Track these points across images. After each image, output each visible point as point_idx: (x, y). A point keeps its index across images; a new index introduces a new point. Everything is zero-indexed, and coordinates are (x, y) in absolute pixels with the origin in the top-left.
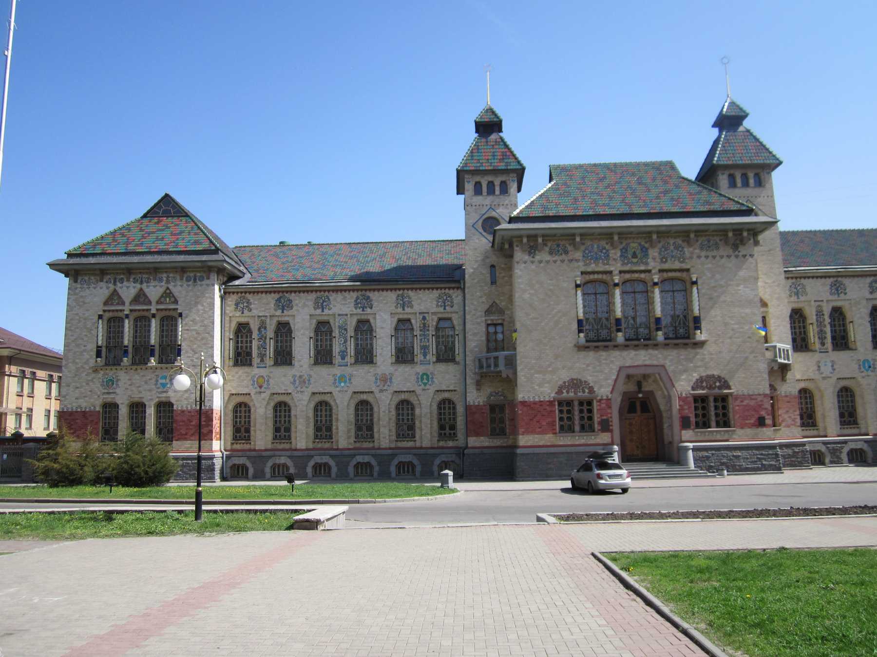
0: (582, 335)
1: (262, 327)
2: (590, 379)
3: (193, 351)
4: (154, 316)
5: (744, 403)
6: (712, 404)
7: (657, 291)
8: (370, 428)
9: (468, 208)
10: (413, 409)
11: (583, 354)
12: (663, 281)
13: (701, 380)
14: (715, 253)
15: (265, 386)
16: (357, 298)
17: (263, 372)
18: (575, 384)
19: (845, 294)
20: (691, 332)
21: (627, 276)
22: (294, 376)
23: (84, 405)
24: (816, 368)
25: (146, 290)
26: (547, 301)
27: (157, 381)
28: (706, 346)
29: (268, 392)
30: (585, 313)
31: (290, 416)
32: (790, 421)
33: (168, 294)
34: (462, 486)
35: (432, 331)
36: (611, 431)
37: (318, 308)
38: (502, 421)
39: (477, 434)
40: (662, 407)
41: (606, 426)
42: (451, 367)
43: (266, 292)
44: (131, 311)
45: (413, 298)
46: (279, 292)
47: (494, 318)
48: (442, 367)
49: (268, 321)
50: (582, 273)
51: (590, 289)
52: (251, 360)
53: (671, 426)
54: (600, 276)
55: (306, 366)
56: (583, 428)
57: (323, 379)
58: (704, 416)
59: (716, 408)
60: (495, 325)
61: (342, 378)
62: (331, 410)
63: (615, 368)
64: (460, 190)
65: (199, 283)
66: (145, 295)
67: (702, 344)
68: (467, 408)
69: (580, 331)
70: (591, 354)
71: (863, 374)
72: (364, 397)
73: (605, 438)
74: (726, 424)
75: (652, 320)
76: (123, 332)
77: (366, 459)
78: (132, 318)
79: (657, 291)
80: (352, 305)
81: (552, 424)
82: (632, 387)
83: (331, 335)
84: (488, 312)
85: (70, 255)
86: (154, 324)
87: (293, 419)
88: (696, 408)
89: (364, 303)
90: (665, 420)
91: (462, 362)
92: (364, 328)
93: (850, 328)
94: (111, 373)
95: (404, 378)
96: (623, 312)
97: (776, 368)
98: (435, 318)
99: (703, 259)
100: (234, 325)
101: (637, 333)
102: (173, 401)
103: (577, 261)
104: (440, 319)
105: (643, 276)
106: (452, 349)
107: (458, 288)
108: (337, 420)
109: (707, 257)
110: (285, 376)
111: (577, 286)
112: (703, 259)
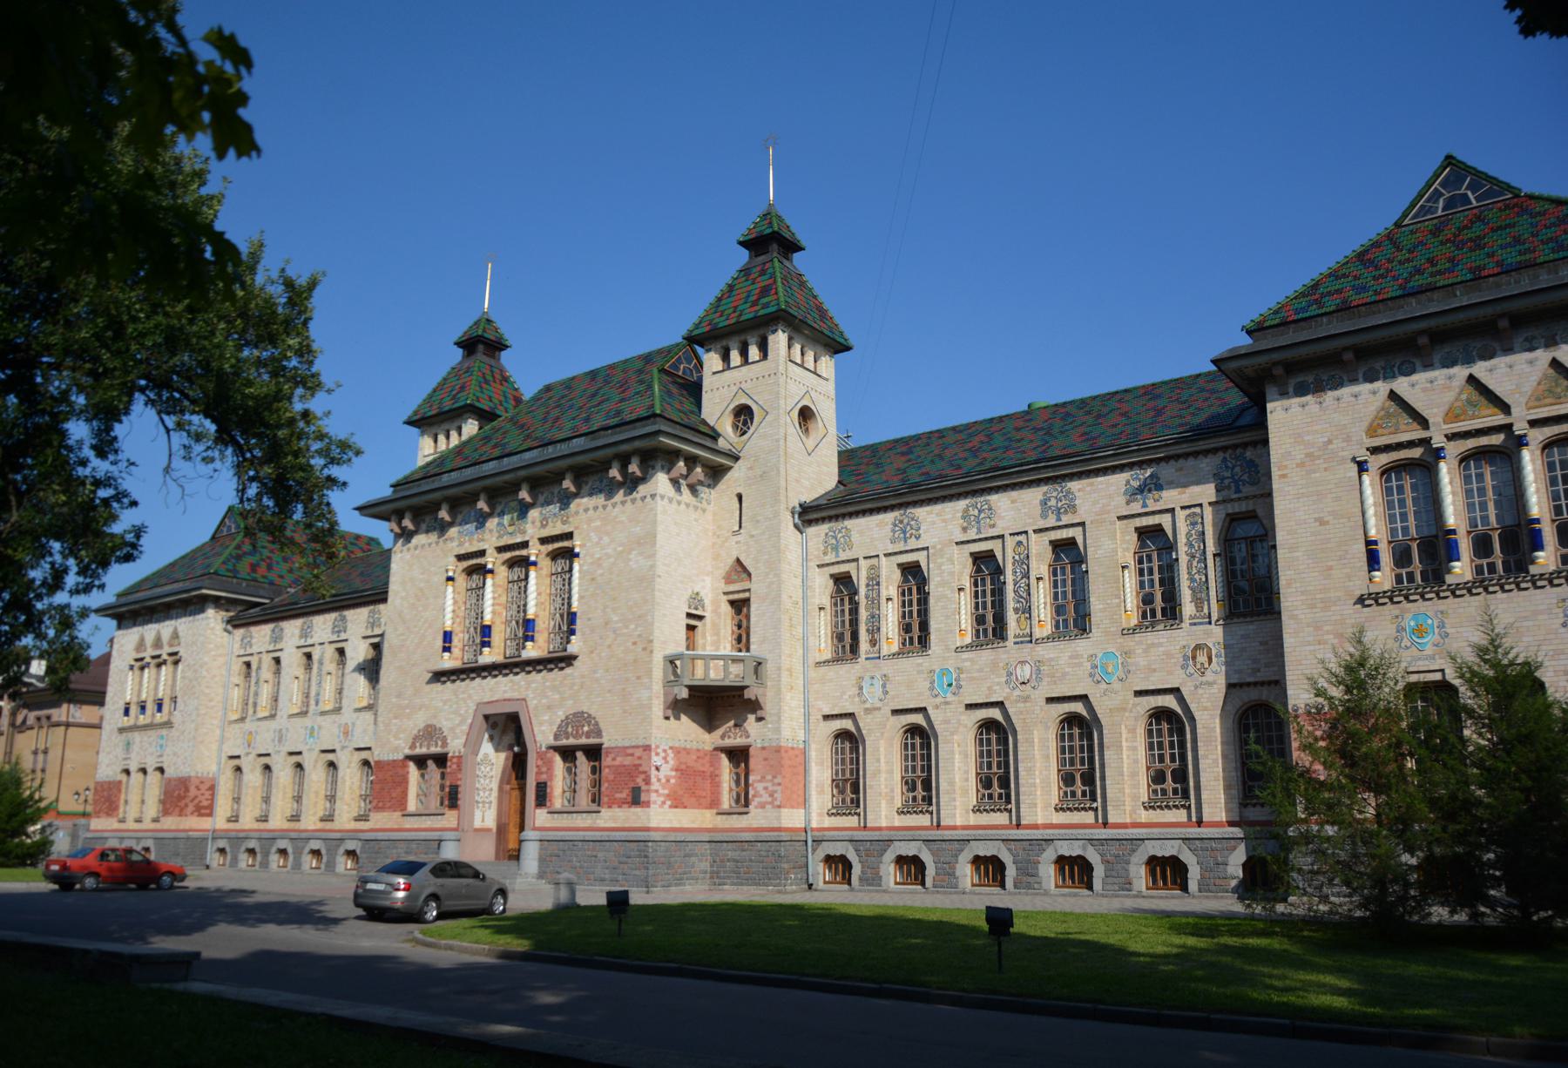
2: (445, 724)
5: (617, 763)
13: (567, 721)
18: (430, 732)
19: (918, 538)
24: (855, 690)
28: (576, 663)
32: (766, 798)
71: (939, 700)
85: (119, 596)
99: (591, 512)
103: (452, 539)
109: (596, 508)
111: (450, 579)
112: (591, 512)
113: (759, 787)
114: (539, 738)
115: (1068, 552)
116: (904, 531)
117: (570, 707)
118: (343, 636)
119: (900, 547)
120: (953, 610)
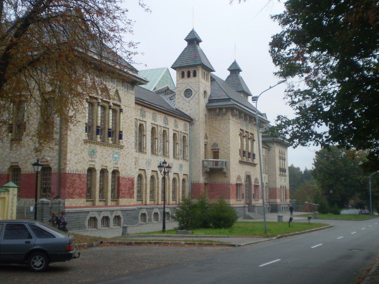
2: (241, 176)
3: (127, 136)
23: (80, 169)
27: (113, 155)
45: (179, 123)
63: (244, 172)
65: (129, 91)
80: (163, 121)
89: (166, 122)
94: (93, 146)
102: (120, 170)
107: (189, 122)
110: (143, 159)
118: (167, 127)
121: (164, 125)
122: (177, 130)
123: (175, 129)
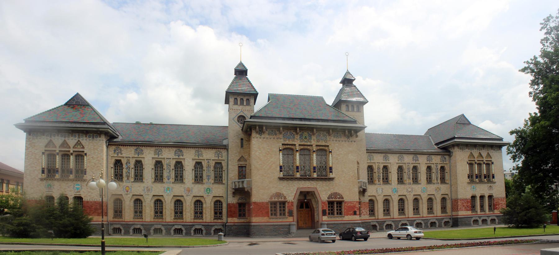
0: (281, 173)
1: (128, 162)
2: (285, 193)
4: (72, 154)
6: (335, 205)
7: (315, 155)
8: (181, 213)
9: (231, 110)
10: (202, 204)
11: (282, 182)
12: (318, 150)
13: (331, 195)
14: (338, 139)
15: (129, 191)
16: (176, 151)
17: (129, 184)
18: (278, 195)
20: (328, 173)
21: (302, 147)
22: (144, 187)
25: (68, 141)
26: (266, 156)
29: (131, 195)
30: (283, 163)
31: (142, 206)
32: (365, 213)
33: (79, 143)
34: (228, 240)
35: (212, 168)
36: (293, 216)
37: (156, 154)
38: (244, 210)
39: (232, 216)
40: (314, 206)
41: (291, 214)
42: (221, 186)
43: (130, 146)
44: (74, 151)
46: (136, 146)
47: (242, 163)
48: (216, 186)
49: (131, 159)
50: (283, 144)
51: (286, 152)
52: (122, 179)
53: (318, 214)
54: (290, 147)
55: (150, 182)
56: (281, 214)
57: (159, 189)
58: (332, 210)
59: (337, 207)
60: (242, 167)
61: (168, 189)
62: (162, 204)
64: (227, 102)
66: (67, 143)
67: (332, 179)
68: (228, 205)
69: (281, 171)
70: (285, 181)
72: (179, 198)
73: (291, 219)
74: (341, 214)
75: (312, 168)
76: (55, 161)
77: (179, 227)
78: (60, 154)
79: (315, 155)
81: (268, 213)
82: (302, 198)
83: (162, 168)
84: (239, 160)
86: (72, 158)
87: (144, 207)
88: (329, 207)
90: (315, 212)
91: (226, 184)
92: (179, 165)
93: (390, 175)
95: (198, 190)
96: (300, 163)
97: (362, 190)
98: (214, 162)
100: (113, 161)
101: (305, 173)
104: (216, 163)
105: (309, 147)
106: (221, 177)
108: (165, 208)
111: (280, 150)
113: (363, 211)
114: (322, 198)
115: (415, 168)
116: (386, 158)
117: (332, 191)
118: (181, 157)
119: (385, 162)
120: (394, 176)
121: (177, 157)
122: (200, 158)
123: (197, 158)
